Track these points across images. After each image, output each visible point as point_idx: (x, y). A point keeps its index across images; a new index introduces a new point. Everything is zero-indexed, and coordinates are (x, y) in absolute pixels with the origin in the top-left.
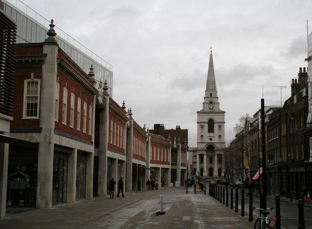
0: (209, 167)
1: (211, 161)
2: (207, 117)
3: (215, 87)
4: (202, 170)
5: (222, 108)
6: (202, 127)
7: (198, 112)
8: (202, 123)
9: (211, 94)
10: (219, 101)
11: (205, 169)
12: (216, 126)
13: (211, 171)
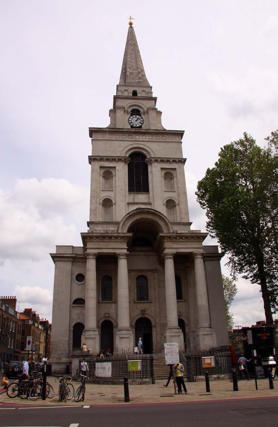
0: (138, 315)
1: (142, 290)
2: (126, 144)
5: (168, 123)
6: (108, 174)
7: (93, 132)
9: (135, 93)
12: (155, 172)
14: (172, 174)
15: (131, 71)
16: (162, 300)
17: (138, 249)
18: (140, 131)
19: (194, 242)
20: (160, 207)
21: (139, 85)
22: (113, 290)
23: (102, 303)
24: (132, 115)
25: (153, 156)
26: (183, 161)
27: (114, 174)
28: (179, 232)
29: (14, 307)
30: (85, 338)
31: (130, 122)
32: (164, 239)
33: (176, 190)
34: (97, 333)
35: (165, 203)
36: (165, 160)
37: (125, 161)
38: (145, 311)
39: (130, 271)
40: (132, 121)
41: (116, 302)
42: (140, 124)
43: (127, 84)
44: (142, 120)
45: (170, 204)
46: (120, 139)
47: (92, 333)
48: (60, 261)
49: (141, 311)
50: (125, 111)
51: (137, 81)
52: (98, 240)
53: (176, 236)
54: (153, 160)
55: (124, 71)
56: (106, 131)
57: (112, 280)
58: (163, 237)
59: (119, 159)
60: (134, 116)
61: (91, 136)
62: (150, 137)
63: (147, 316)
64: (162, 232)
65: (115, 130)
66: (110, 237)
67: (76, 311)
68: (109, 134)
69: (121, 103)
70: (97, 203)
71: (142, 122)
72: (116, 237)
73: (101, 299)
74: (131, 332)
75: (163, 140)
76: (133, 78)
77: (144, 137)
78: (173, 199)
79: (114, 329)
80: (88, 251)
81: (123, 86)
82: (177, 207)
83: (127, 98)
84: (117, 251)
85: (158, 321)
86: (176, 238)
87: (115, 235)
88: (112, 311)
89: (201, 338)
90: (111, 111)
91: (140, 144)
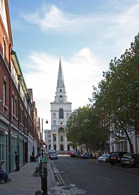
3: (64, 85)
4: (55, 147)
5: (69, 100)
6: (54, 114)
7: (51, 103)
9: (61, 90)
11: (58, 146)
12: (65, 114)
13: (62, 147)
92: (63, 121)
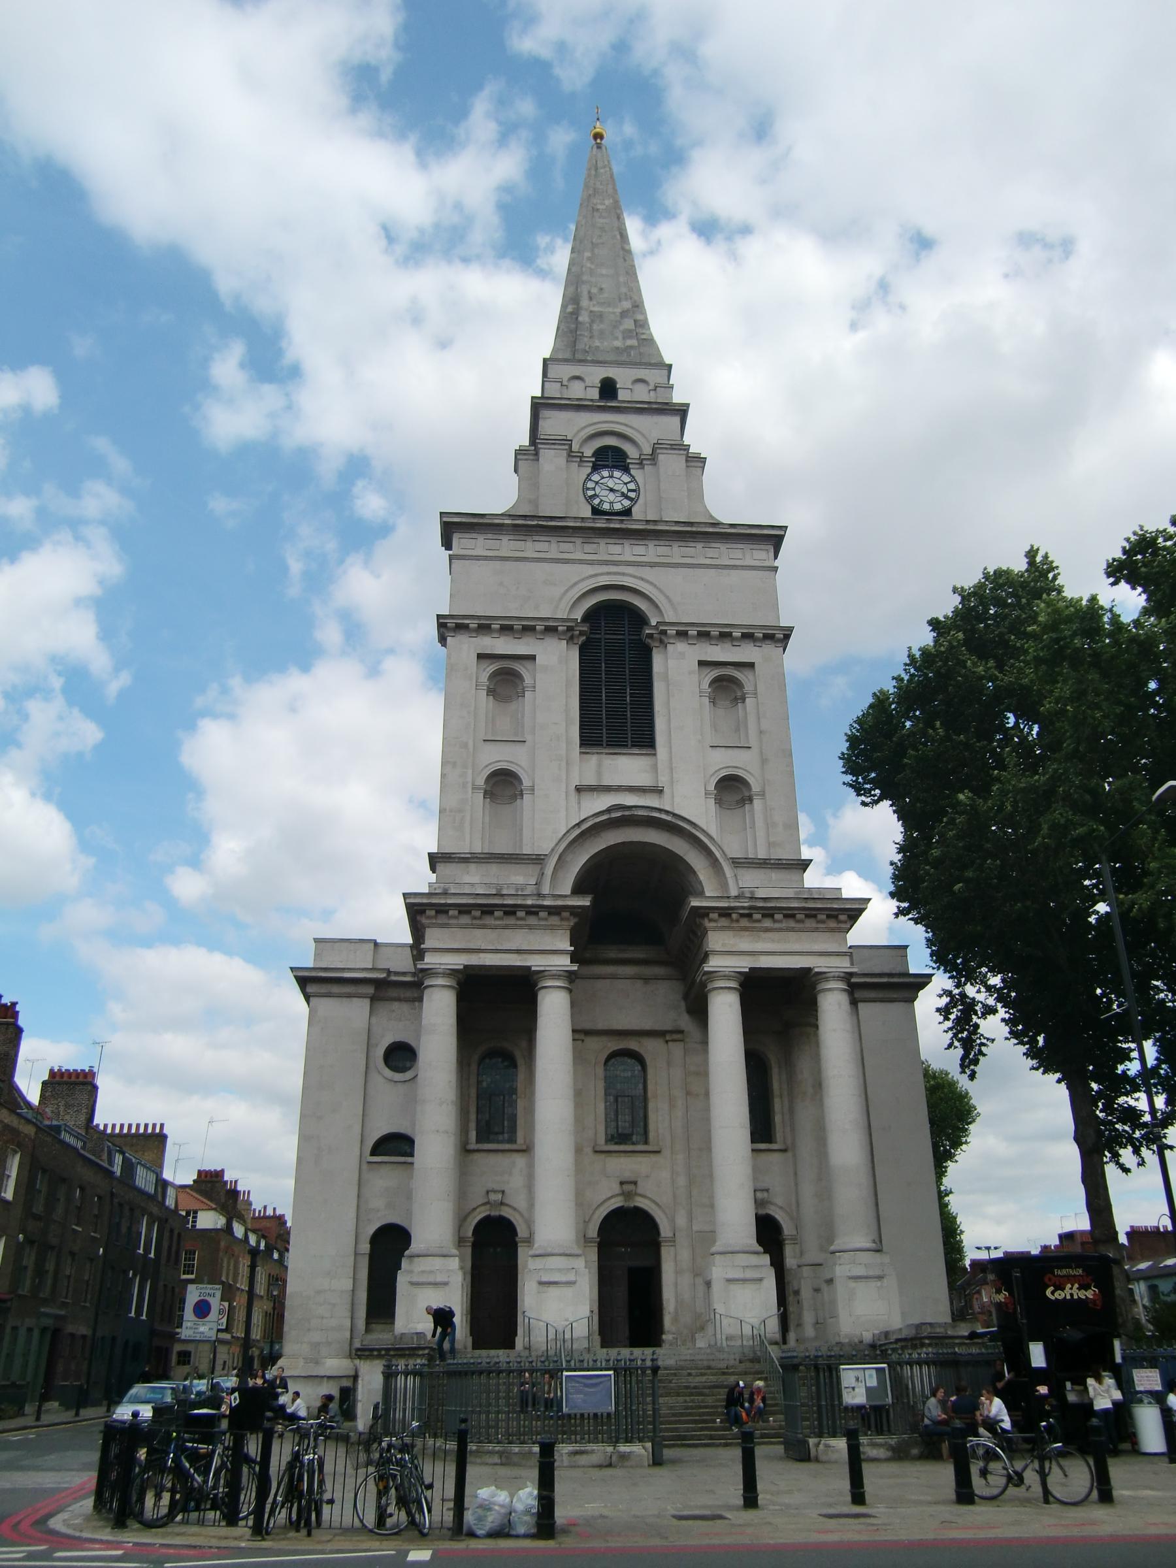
0: (606, 1197)
5: (727, 499)
6: (506, 679)
7: (453, 528)
8: (506, 629)
9: (608, 389)
10: (695, 437)
12: (677, 676)
13: (628, 1250)
14: (517, 676)
15: (596, 309)
16: (699, 1143)
17: (612, 954)
18: (623, 526)
19: (816, 930)
20: (691, 800)
21: (624, 358)
22: (521, 1104)
23: (478, 1151)
24: (596, 468)
25: (670, 617)
26: (780, 637)
27: (528, 680)
28: (760, 894)
29: (157, 1165)
30: (412, 1284)
31: (590, 493)
32: (706, 920)
33: (753, 741)
34: (454, 1263)
35: (711, 787)
36: (715, 632)
37: (569, 634)
38: (635, 1183)
39: (580, 1033)
40: (598, 490)
41: (527, 1150)
42: (627, 503)
43: (579, 356)
44: (632, 486)
45: (732, 789)
46: (554, 554)
47: (437, 1263)
48: (328, 995)
49: (622, 1183)
50: (570, 454)
51: (618, 343)
52: (465, 919)
53: (750, 908)
54: (672, 631)
55: (570, 309)
56: (502, 525)
57: (515, 1066)
58: (704, 912)
59: (550, 630)
60: (605, 473)
61: (447, 544)
62: (662, 550)
63: (641, 1203)
64: (701, 894)
65: (535, 523)
66: (510, 911)
67: (384, 1178)
68: (512, 537)
69: (555, 424)
70: (464, 785)
71: (632, 495)
72: (532, 911)
73: (473, 1135)
74: (580, 1263)
75: (708, 561)
76: (602, 332)
77: (640, 550)
78: (740, 773)
79: (522, 1252)
80: (430, 960)
81: (566, 360)
82: (757, 803)
83: (579, 407)
84: (536, 962)
85: (681, 1221)
86: (749, 916)
87: (529, 902)
88: (515, 1183)
89: (841, 1290)
90: (519, 453)
91: (624, 574)
92: (644, 780)
